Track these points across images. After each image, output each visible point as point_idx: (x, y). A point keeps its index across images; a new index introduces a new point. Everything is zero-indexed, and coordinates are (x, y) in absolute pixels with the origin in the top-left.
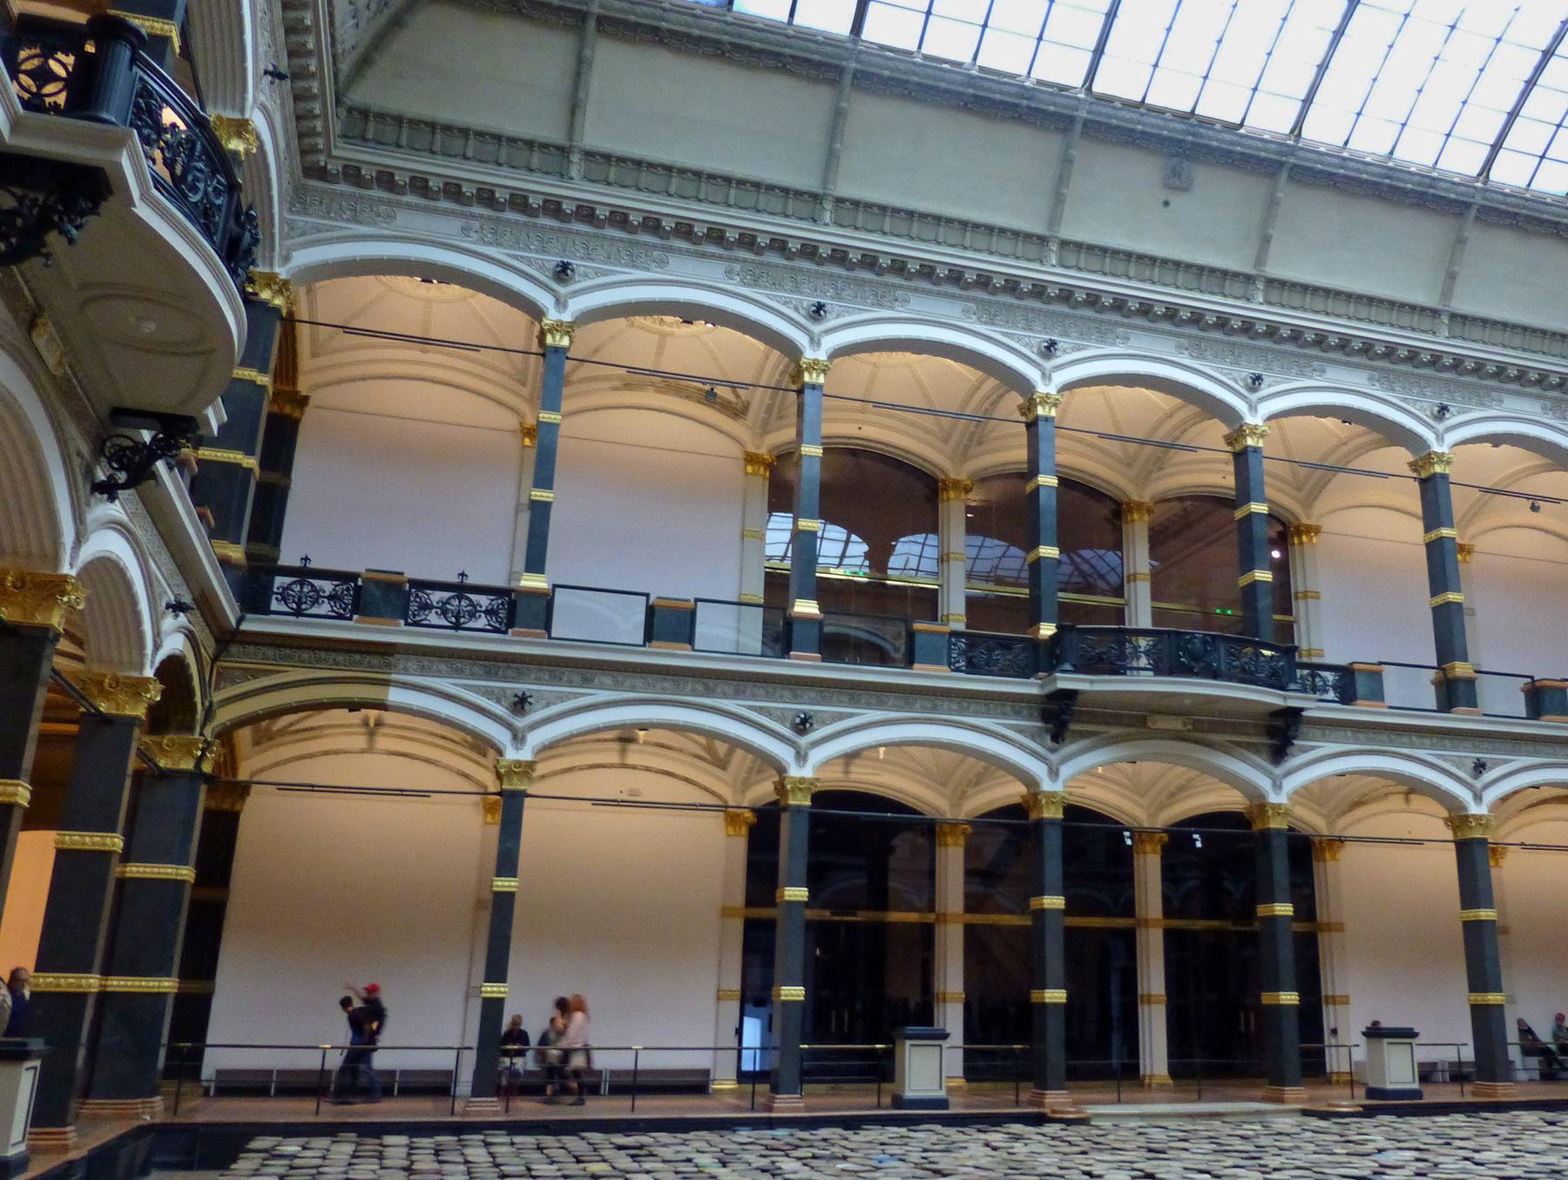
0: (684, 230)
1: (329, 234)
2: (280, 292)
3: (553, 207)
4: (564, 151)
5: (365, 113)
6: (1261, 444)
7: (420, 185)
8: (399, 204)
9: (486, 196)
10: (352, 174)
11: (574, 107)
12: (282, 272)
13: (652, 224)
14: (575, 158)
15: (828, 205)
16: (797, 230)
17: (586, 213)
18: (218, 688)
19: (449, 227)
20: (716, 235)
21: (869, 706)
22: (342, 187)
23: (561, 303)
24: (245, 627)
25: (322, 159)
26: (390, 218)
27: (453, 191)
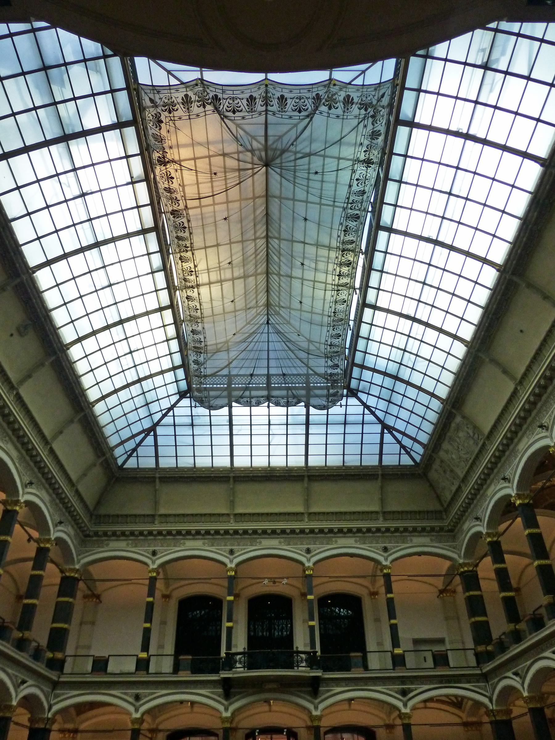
0: (188, 533)
1: (90, 553)
2: (76, 573)
3: (150, 533)
4: (153, 516)
5: (100, 516)
6: (390, 571)
7: (114, 534)
8: (110, 540)
9: (132, 533)
10: (96, 534)
11: (156, 503)
12: (77, 567)
13: (179, 533)
14: (157, 517)
16: (222, 527)
17: (160, 533)
18: (54, 700)
19: (122, 544)
20: (198, 532)
21: (162, 689)
22: (95, 538)
23: (153, 562)
24: (61, 679)
25: (88, 532)
26: (107, 545)
27: (123, 534)
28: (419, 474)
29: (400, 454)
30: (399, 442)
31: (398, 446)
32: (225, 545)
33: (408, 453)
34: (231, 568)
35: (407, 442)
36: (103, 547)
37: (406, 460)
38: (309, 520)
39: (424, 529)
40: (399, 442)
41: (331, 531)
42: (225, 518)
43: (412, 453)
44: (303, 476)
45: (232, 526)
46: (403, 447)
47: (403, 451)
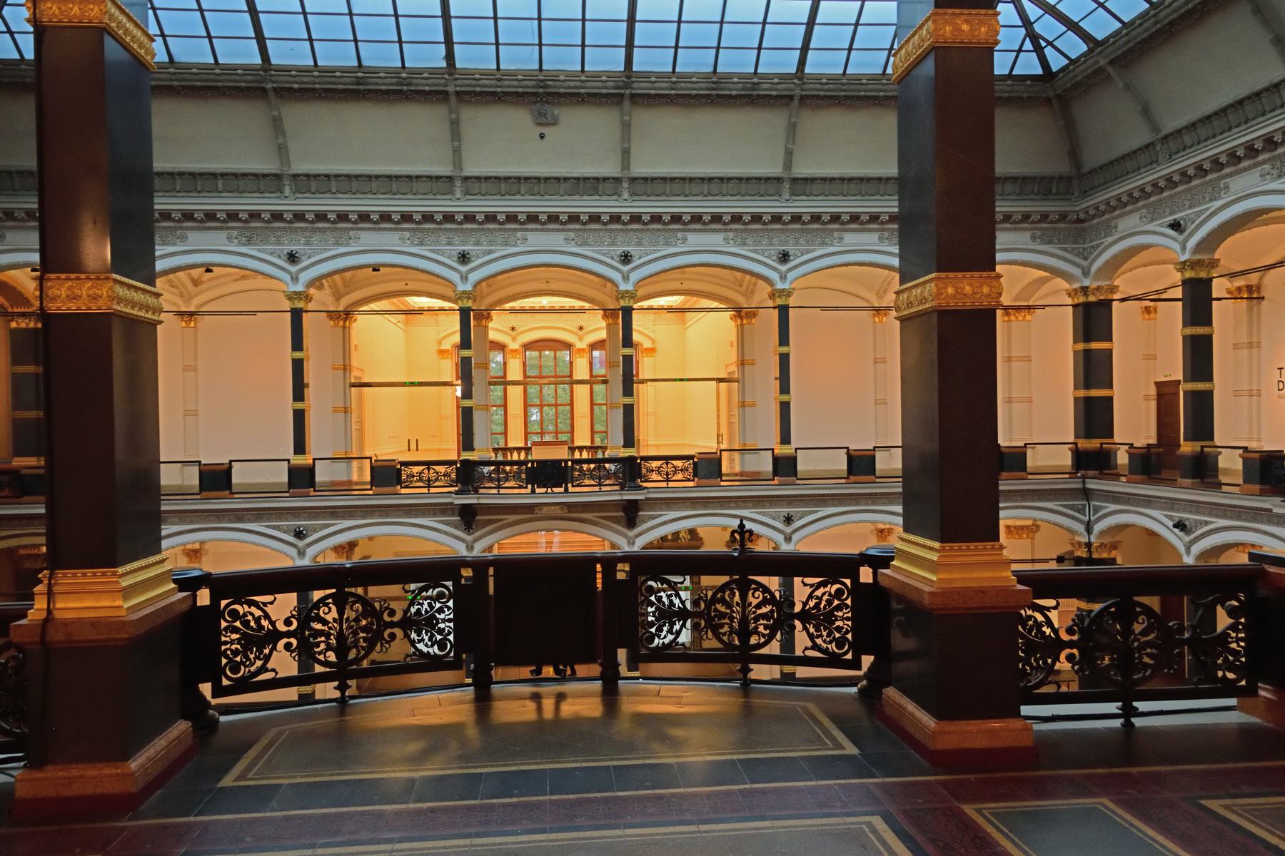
15: (625, 185)
20: (553, 218)
28: (1048, 100)
29: (1020, 51)
30: (1027, 23)
31: (1023, 31)
32: (613, 244)
33: (1039, 50)
34: (627, 292)
35: (1047, 27)
36: (348, 245)
37: (1029, 65)
38: (792, 194)
39: (1026, 217)
40: (1027, 23)
41: (835, 218)
42: (608, 186)
43: (1049, 51)
44: (791, 98)
45: (625, 205)
46: (1034, 37)
47: (1028, 45)
